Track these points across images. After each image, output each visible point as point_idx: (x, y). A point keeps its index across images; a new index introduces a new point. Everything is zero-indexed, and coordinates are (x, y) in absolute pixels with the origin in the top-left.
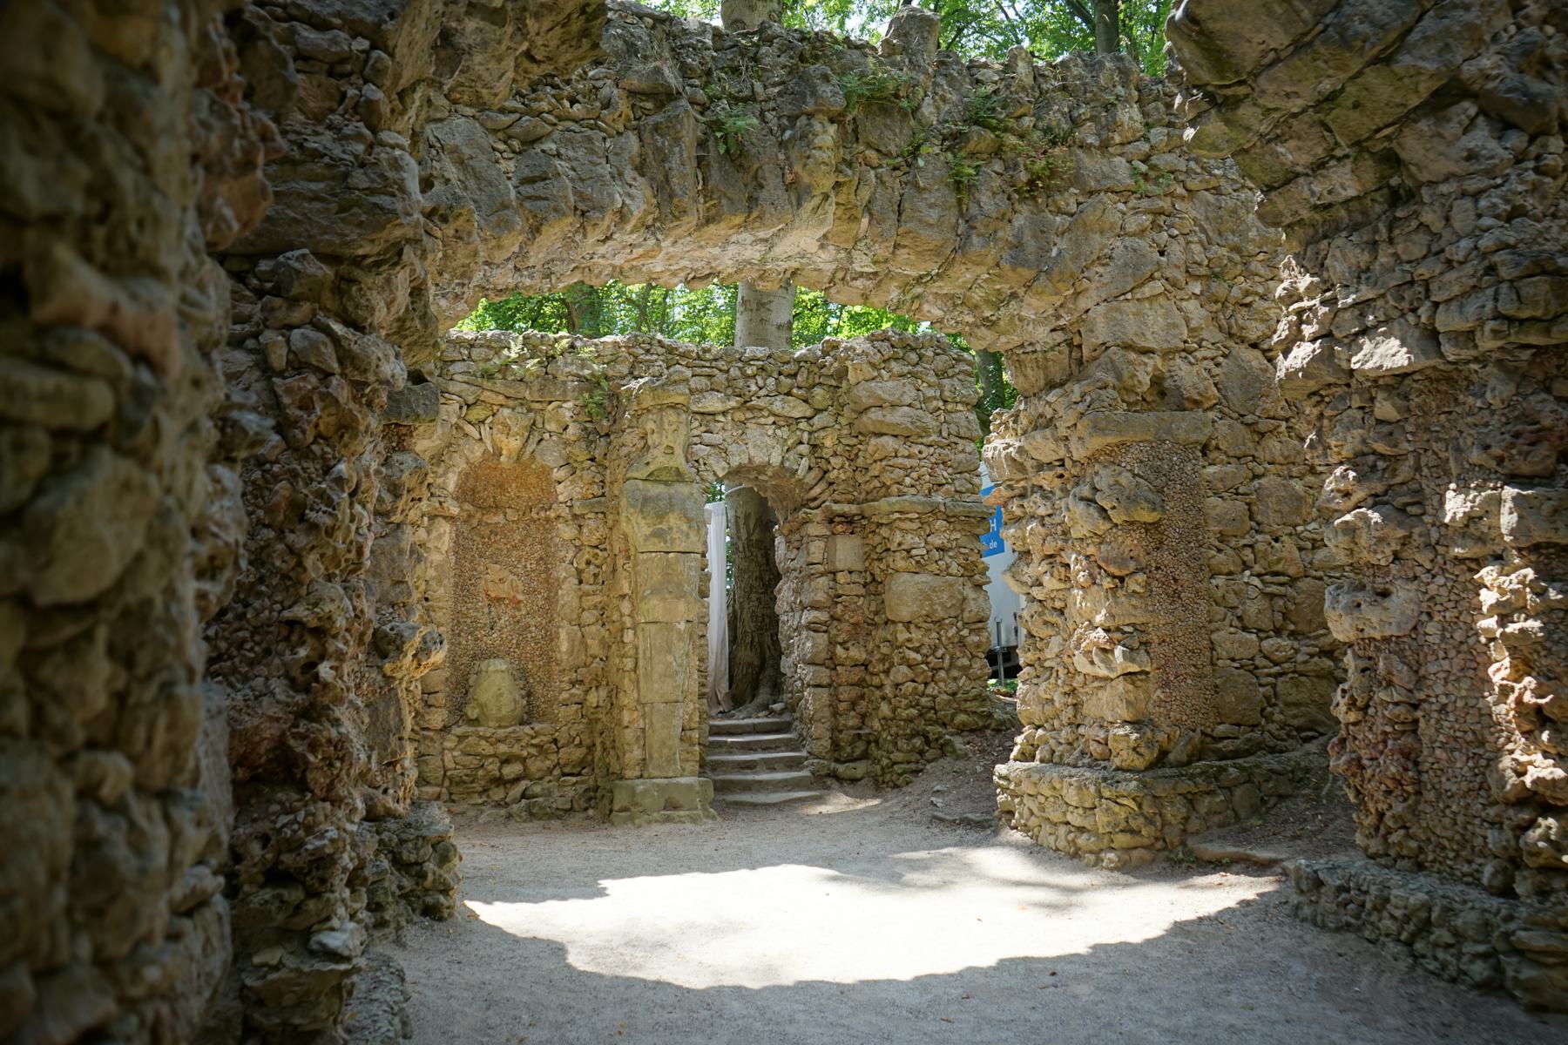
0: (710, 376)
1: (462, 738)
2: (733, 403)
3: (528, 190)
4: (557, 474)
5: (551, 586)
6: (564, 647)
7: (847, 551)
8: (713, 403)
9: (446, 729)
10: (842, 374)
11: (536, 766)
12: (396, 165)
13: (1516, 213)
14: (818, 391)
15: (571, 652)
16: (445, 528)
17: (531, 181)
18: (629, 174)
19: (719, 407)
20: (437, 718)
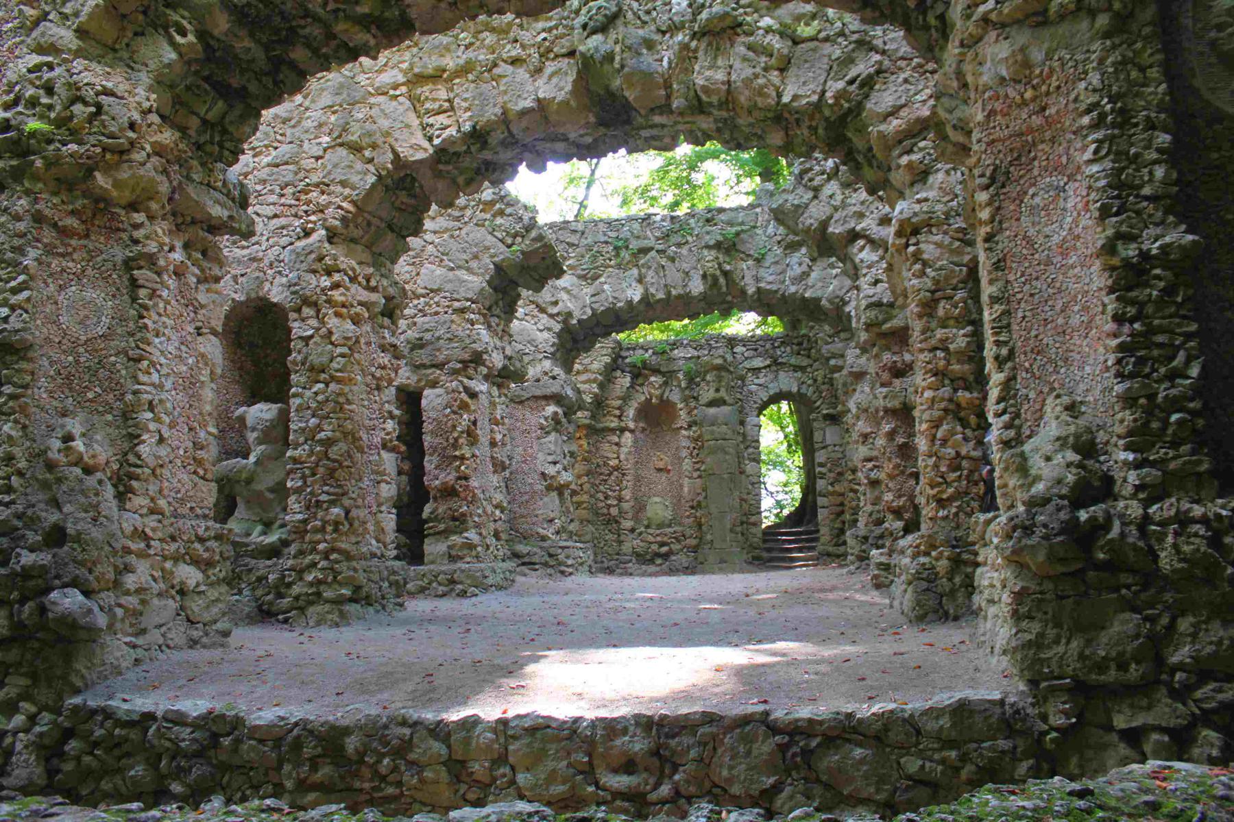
0: (756, 350)
1: (640, 534)
2: (768, 362)
3: (593, 299)
4: (680, 406)
5: (681, 460)
6: (686, 489)
7: (830, 434)
8: (758, 363)
9: (632, 530)
10: (816, 342)
11: (676, 547)
12: (478, 334)
13: (877, 282)
14: (813, 351)
15: (689, 492)
16: (627, 434)
17: (593, 296)
18: (634, 284)
19: (762, 365)
20: (628, 524)
